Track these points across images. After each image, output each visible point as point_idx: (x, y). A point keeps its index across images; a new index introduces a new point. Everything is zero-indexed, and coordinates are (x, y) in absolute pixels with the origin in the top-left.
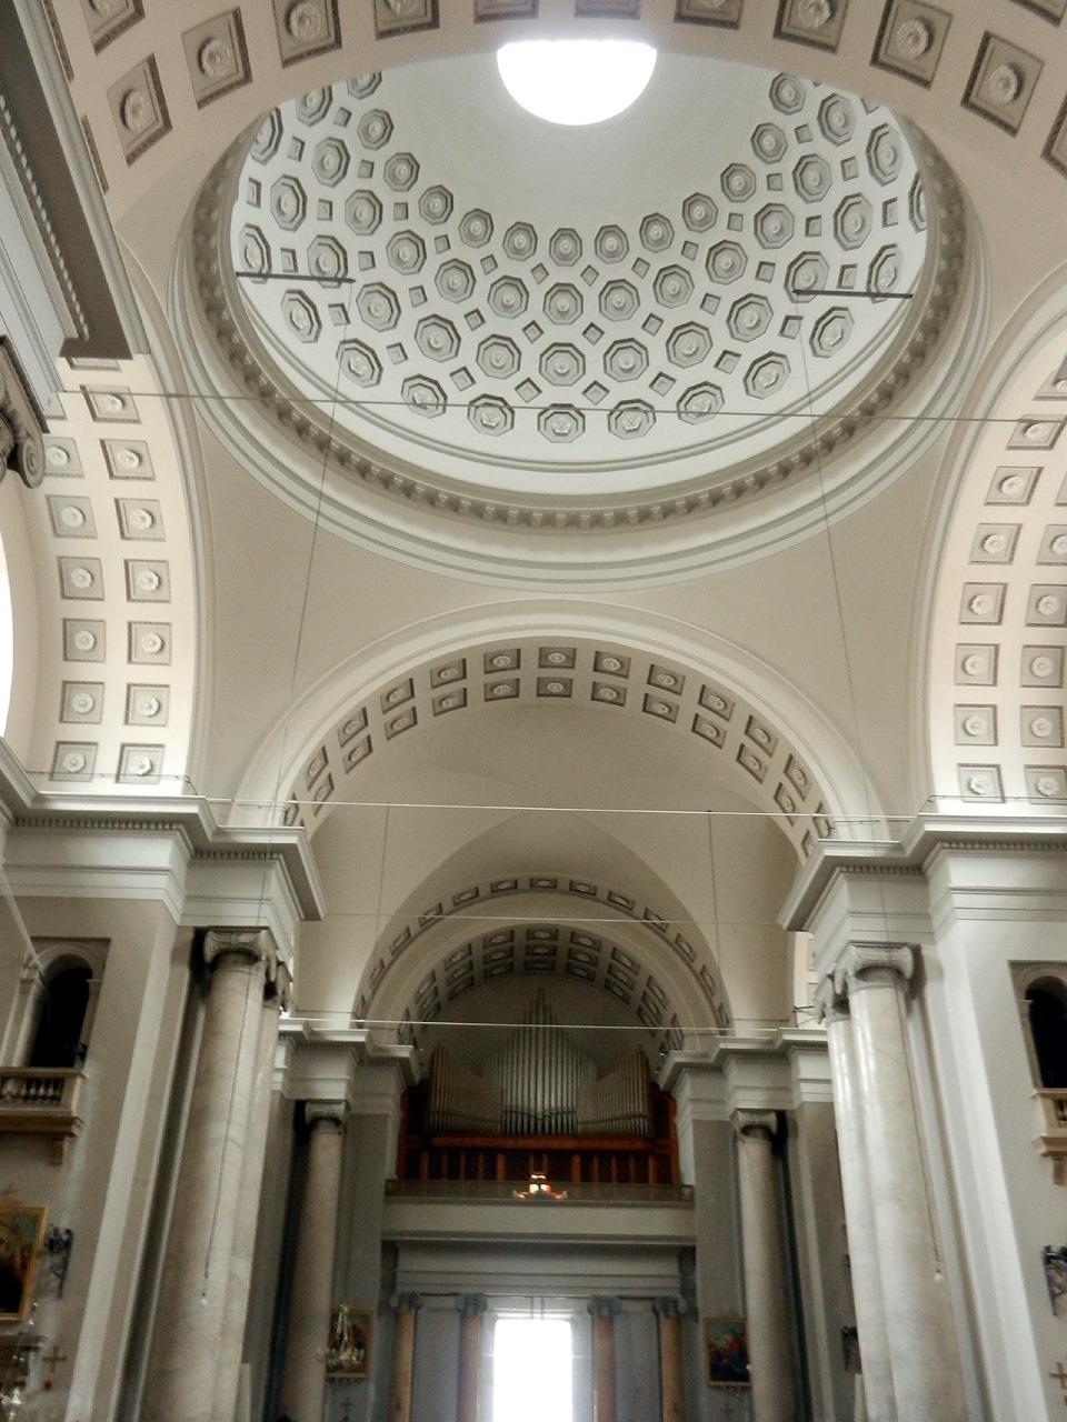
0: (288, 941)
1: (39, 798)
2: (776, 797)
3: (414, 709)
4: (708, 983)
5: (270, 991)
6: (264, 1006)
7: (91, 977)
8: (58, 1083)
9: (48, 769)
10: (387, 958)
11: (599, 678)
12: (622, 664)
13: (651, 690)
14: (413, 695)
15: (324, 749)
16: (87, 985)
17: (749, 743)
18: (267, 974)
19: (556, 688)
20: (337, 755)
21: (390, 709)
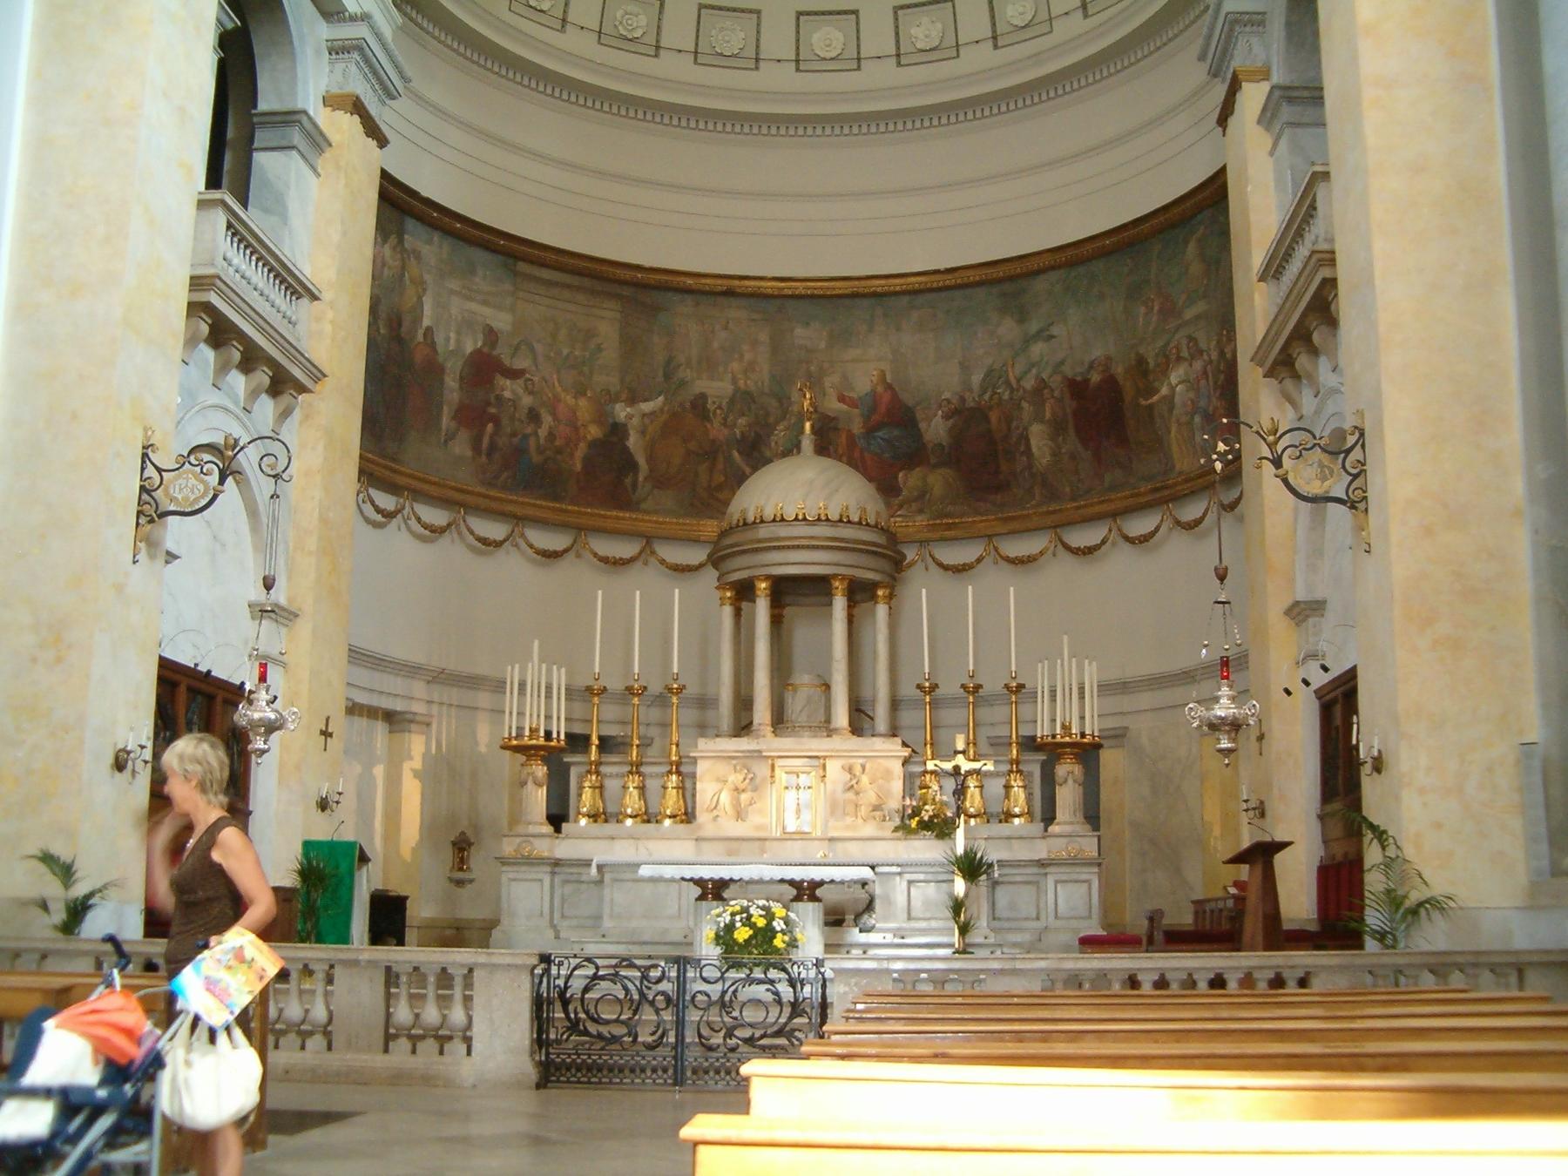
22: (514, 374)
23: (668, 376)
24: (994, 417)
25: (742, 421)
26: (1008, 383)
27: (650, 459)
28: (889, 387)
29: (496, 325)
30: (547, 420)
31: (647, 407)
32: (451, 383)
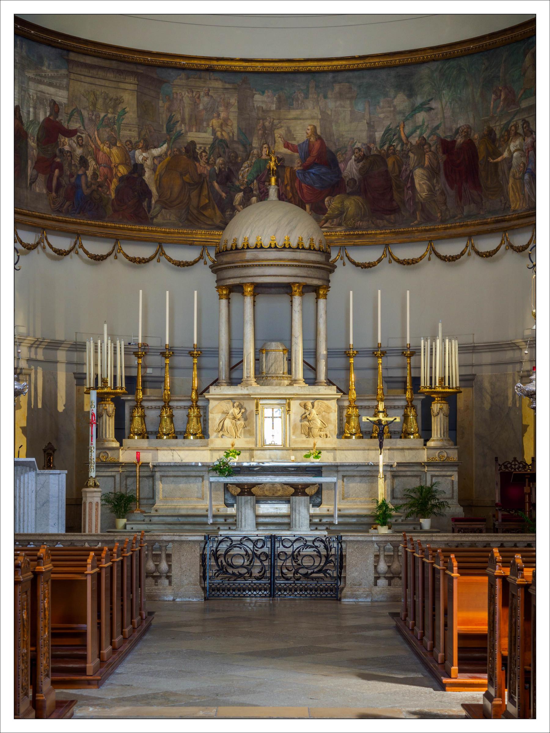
23: (169, 130)
24: (390, 161)
25: (219, 161)
27: (159, 187)
28: (319, 138)
29: (57, 99)
30: (92, 163)
31: (156, 152)
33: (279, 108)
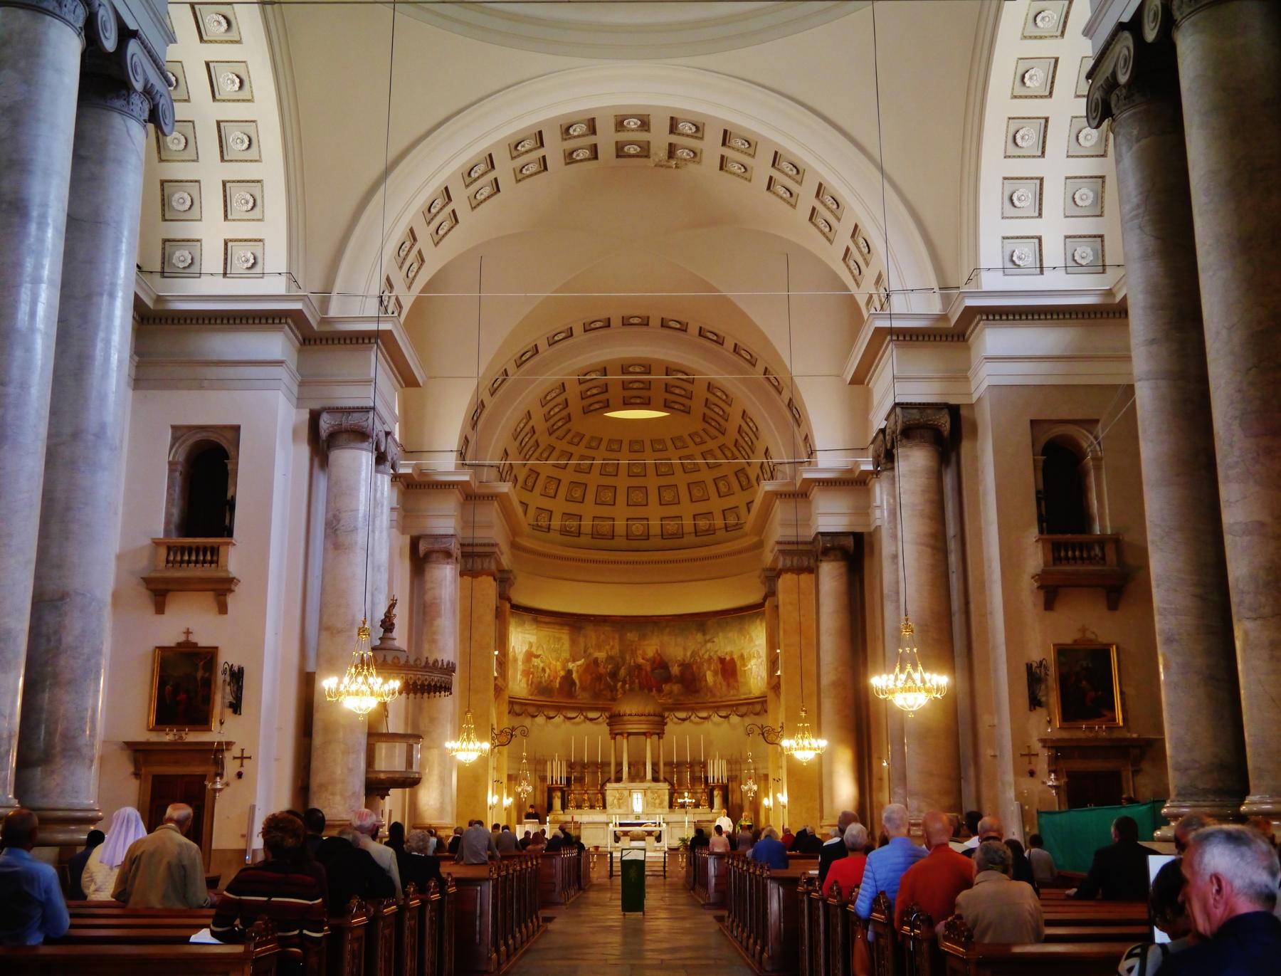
0: (392, 412)
1: (159, 299)
2: (844, 259)
3: (496, 180)
4: (795, 412)
5: (381, 459)
6: (377, 471)
7: (228, 459)
8: (215, 551)
9: (159, 269)
10: (486, 397)
11: (674, 139)
12: (697, 128)
13: (726, 152)
14: (493, 167)
15: (412, 231)
16: (226, 465)
17: (819, 207)
18: (377, 448)
19: (632, 150)
20: (424, 234)
21: (472, 183)
22: (537, 656)
23: (585, 652)
24: (694, 667)
25: (610, 666)
26: (699, 656)
28: (659, 655)
30: (548, 671)
31: (579, 663)
32: (520, 663)
33: (639, 639)
